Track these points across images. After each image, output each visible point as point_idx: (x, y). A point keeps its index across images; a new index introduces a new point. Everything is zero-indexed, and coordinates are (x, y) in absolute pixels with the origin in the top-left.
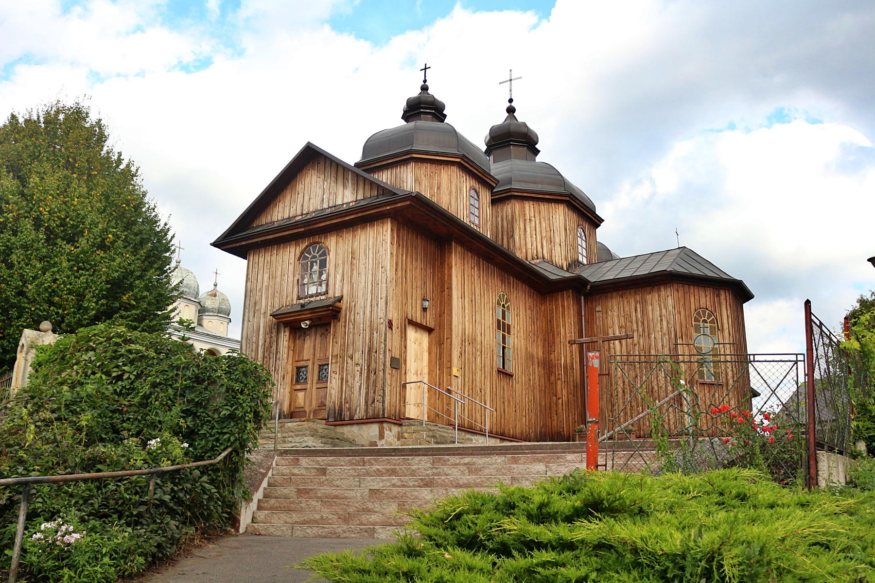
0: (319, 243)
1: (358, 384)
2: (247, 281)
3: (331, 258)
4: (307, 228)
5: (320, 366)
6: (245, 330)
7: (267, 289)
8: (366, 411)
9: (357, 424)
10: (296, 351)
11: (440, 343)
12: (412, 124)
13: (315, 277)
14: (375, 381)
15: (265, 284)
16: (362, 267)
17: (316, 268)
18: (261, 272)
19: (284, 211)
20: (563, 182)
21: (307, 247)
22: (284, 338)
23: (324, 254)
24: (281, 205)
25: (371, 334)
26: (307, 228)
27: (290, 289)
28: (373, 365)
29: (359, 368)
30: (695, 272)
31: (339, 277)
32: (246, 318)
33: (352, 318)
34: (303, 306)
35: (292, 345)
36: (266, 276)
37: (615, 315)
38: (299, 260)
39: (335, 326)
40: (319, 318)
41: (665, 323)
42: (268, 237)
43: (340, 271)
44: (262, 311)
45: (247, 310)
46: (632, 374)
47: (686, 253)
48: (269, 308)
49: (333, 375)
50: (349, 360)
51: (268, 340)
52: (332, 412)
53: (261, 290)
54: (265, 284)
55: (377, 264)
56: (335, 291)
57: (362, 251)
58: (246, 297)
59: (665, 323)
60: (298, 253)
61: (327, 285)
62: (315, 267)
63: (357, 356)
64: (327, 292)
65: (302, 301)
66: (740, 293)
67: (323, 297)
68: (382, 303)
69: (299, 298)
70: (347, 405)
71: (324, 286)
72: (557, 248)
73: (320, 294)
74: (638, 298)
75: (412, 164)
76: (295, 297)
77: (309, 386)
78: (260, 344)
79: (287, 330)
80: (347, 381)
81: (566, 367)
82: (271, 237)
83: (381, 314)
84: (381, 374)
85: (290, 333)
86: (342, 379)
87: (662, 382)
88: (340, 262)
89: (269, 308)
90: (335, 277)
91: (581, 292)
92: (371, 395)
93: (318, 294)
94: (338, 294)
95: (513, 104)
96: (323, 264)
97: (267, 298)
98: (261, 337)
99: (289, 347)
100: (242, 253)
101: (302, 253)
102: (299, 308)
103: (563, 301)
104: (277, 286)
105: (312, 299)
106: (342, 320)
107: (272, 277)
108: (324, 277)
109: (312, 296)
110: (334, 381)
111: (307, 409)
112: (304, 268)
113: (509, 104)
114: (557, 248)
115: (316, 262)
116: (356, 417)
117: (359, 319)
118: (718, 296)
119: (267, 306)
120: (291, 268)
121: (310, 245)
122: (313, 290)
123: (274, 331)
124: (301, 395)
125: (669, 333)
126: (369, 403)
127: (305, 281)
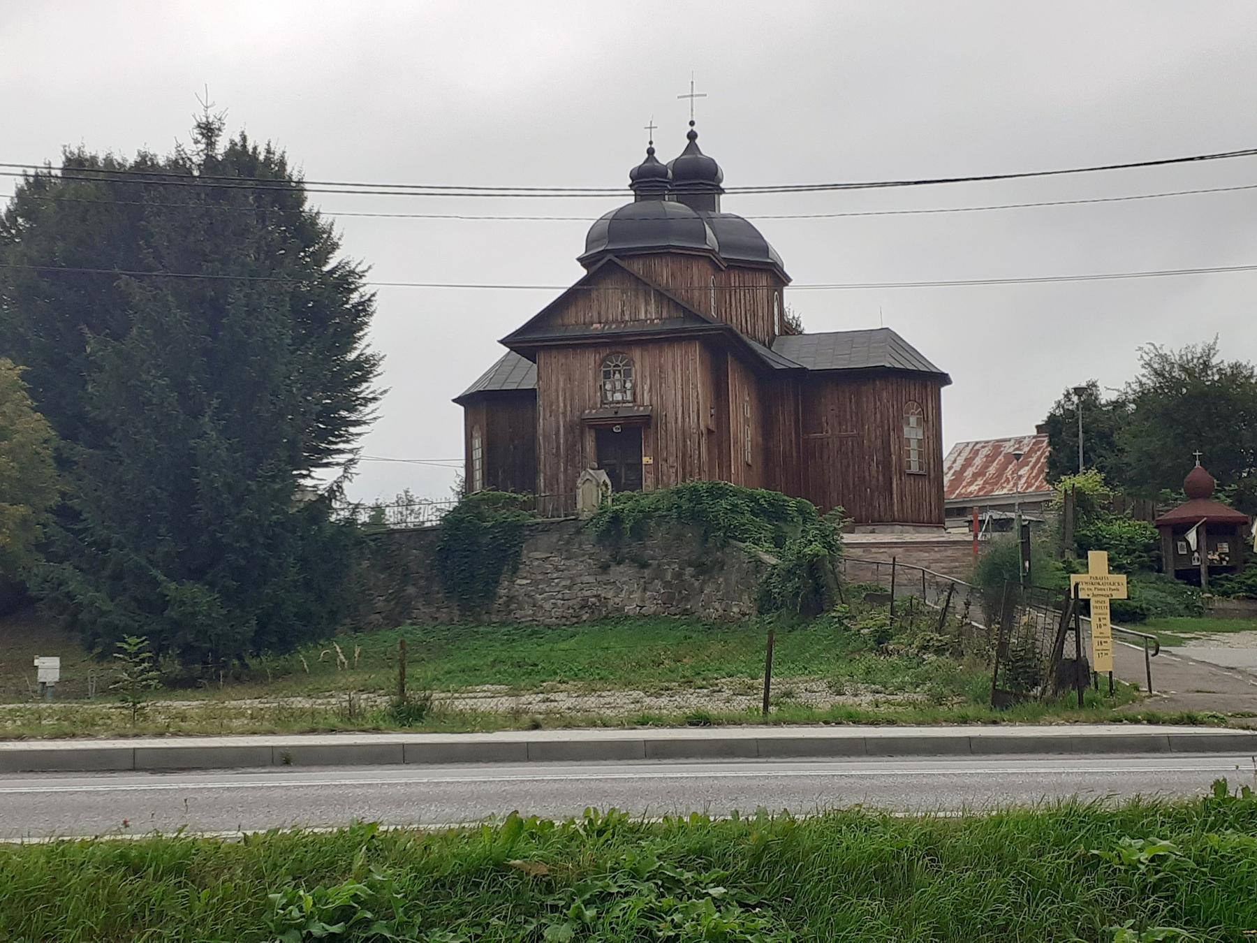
7: (564, 390)
11: (719, 445)
12: (651, 207)
16: (671, 380)
19: (573, 317)
20: (764, 249)
24: (573, 310)
25: (685, 441)
28: (688, 468)
31: (646, 387)
41: (878, 416)
46: (845, 462)
47: (887, 337)
54: (561, 384)
55: (686, 381)
57: (670, 365)
59: (878, 416)
60: (598, 361)
61: (634, 394)
62: (617, 375)
63: (671, 460)
64: (634, 400)
68: (693, 416)
72: (760, 322)
81: (784, 452)
83: (693, 425)
87: (874, 473)
91: (810, 384)
95: (695, 128)
96: (628, 374)
101: (603, 361)
104: (576, 389)
109: (618, 402)
113: (689, 128)
114: (760, 322)
117: (672, 425)
118: (926, 387)
119: (565, 406)
122: (618, 396)
125: (882, 427)
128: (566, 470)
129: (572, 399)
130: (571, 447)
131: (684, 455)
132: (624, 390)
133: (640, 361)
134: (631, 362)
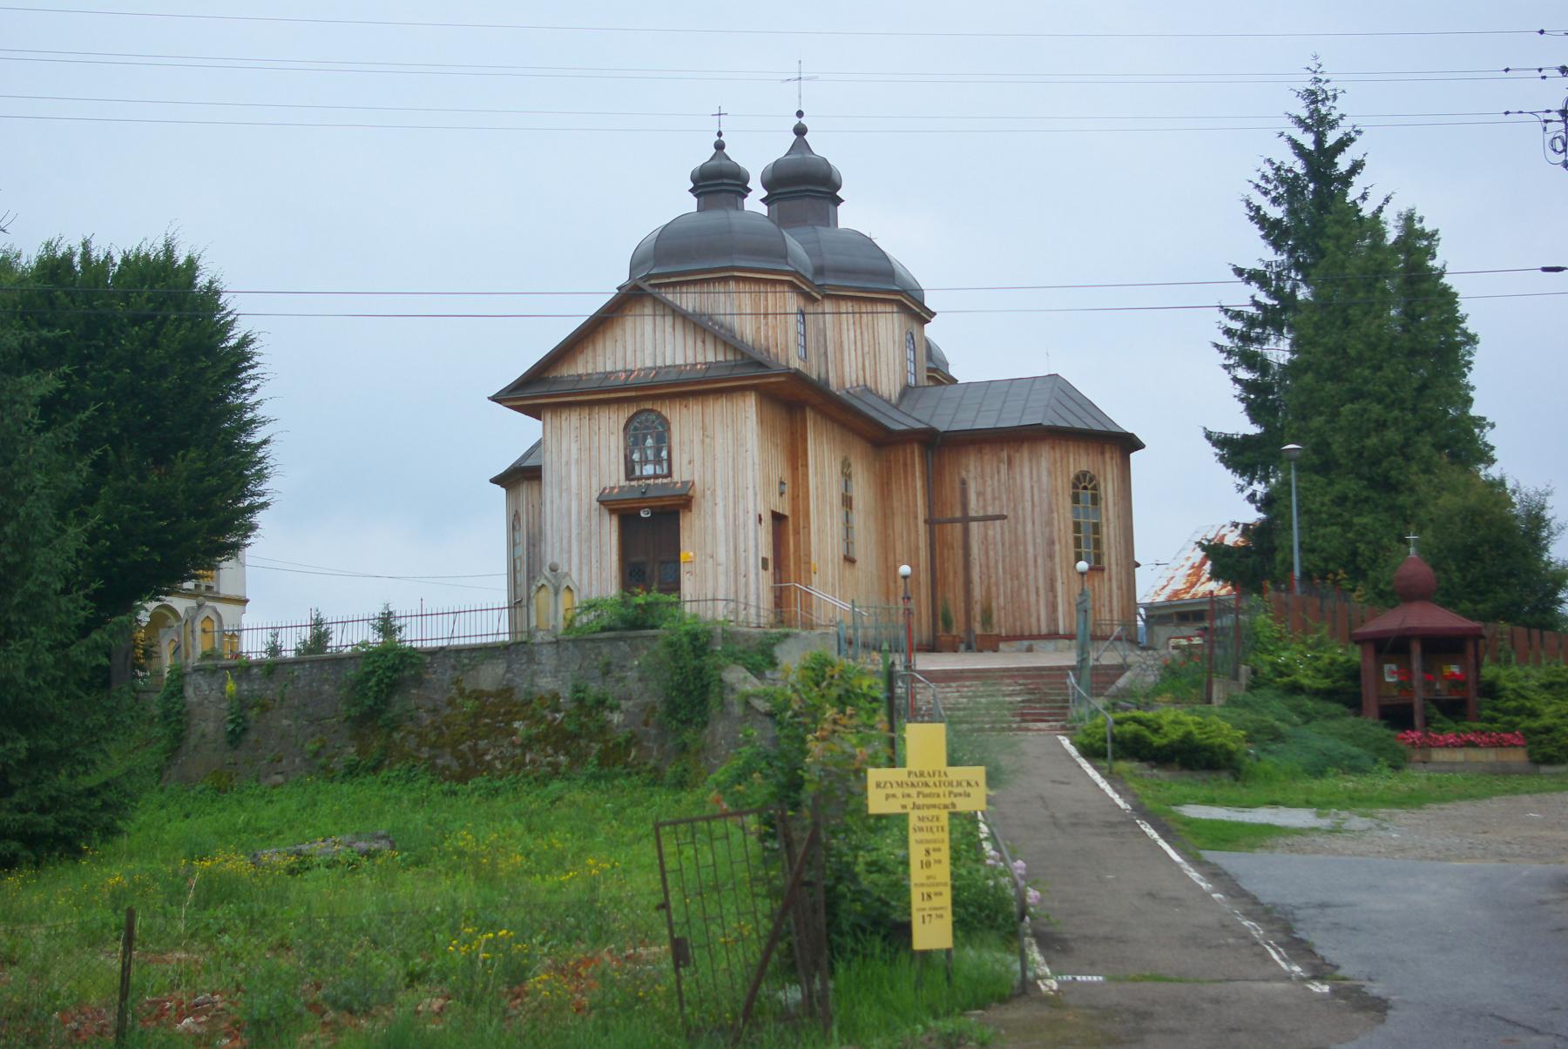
7: (579, 461)
13: (650, 454)
14: (747, 585)
17: (649, 442)
30: (1078, 425)
37: (982, 482)
53: (568, 463)
64: (670, 474)
65: (634, 483)
66: (1128, 444)
71: (665, 465)
74: (1005, 455)
75: (732, 285)
79: (615, 521)
93: (656, 476)
97: (579, 476)
100: (534, 411)
109: (648, 478)
122: (649, 470)
127: (636, 456)
132: (658, 461)
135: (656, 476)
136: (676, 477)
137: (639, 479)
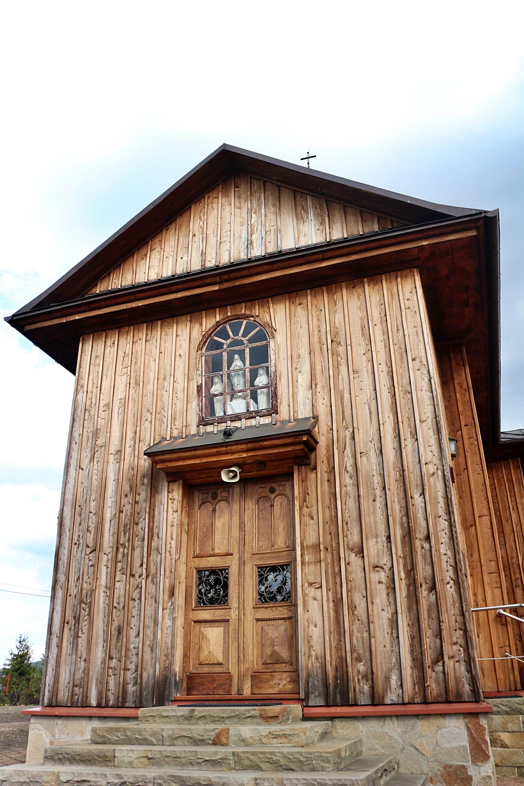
0: (246, 317)
1: (386, 615)
2: (76, 391)
3: (278, 348)
4: (226, 285)
5: (261, 568)
6: (70, 486)
7: (124, 404)
8: (421, 680)
9: (398, 716)
10: (196, 537)
13: (239, 382)
14: (437, 608)
15: (120, 394)
18: (110, 373)
21: (218, 324)
22: (170, 502)
23: (262, 336)
25: (406, 498)
26: (226, 285)
27: (180, 406)
28: (423, 571)
29: (383, 576)
31: (303, 380)
32: (73, 463)
33: (349, 462)
34: (227, 433)
35: (186, 521)
36: (121, 382)
38: (200, 348)
39: (303, 481)
40: (261, 463)
42: (134, 305)
43: (306, 368)
44: (113, 448)
45: (75, 447)
48: (129, 442)
49: (312, 592)
50: (353, 557)
51: (128, 508)
52: (317, 682)
53: (109, 406)
54: (120, 394)
56: (297, 404)
58: (73, 420)
61: (273, 396)
62: (237, 363)
63: (374, 548)
64: (273, 410)
67: (267, 420)
69: (203, 422)
70: (361, 667)
73: (258, 413)
76: (193, 419)
77: (233, 614)
78: (108, 514)
80: (352, 608)
82: (140, 304)
84: (450, 590)
85: (184, 494)
86: (338, 602)
88: (304, 351)
89: (129, 442)
90: (294, 381)
92: (429, 640)
93: (250, 415)
94: (304, 412)
96: (260, 356)
97: (123, 423)
98: (109, 502)
99: (182, 525)
101: (207, 336)
102: (220, 439)
103: (509, 474)
104: (148, 400)
105: (237, 424)
106: (322, 467)
107: (136, 382)
108: (262, 380)
109: (237, 418)
110: (314, 606)
111: (233, 669)
112: (215, 366)
115: (242, 354)
116: (392, 697)
117: (369, 464)
120: (181, 365)
121: (226, 320)
122: (237, 406)
123: (143, 494)
124: (214, 635)
126: (428, 661)
127: (217, 388)
128: (111, 588)
129: (139, 419)
130: (127, 527)
131: (408, 535)
133: (290, 327)
134: (263, 335)
135: (250, 415)
136: (284, 413)
137: (222, 420)
